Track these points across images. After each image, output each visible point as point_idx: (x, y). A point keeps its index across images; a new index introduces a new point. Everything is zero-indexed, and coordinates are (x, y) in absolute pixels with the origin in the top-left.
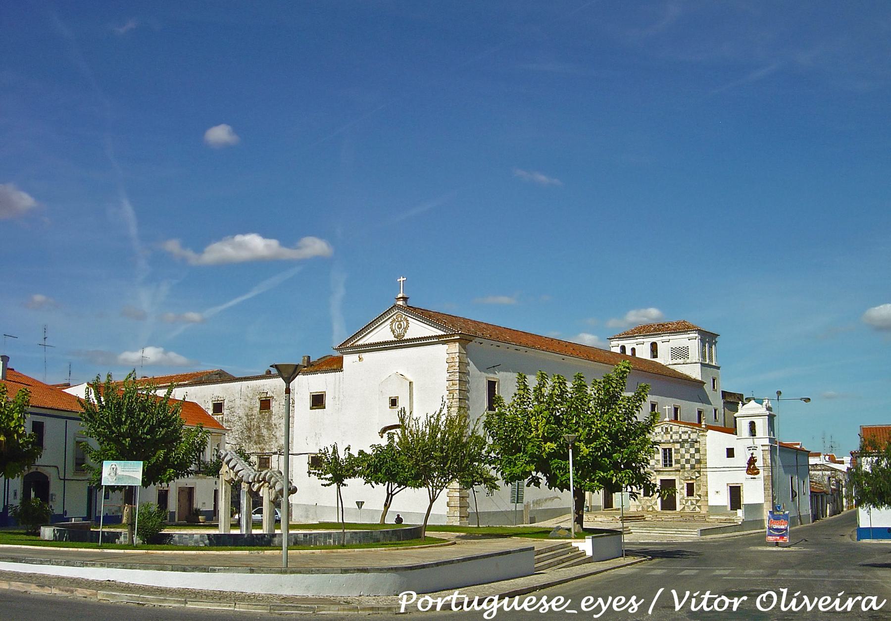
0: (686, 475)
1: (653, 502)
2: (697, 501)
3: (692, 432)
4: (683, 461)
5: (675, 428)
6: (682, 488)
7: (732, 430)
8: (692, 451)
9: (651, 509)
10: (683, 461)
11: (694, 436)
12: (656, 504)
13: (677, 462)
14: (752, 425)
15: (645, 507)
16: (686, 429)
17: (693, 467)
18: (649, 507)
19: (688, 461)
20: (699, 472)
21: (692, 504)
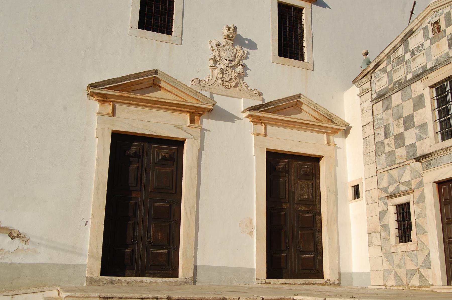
1: (421, 260)
15: (402, 274)
18: (411, 273)
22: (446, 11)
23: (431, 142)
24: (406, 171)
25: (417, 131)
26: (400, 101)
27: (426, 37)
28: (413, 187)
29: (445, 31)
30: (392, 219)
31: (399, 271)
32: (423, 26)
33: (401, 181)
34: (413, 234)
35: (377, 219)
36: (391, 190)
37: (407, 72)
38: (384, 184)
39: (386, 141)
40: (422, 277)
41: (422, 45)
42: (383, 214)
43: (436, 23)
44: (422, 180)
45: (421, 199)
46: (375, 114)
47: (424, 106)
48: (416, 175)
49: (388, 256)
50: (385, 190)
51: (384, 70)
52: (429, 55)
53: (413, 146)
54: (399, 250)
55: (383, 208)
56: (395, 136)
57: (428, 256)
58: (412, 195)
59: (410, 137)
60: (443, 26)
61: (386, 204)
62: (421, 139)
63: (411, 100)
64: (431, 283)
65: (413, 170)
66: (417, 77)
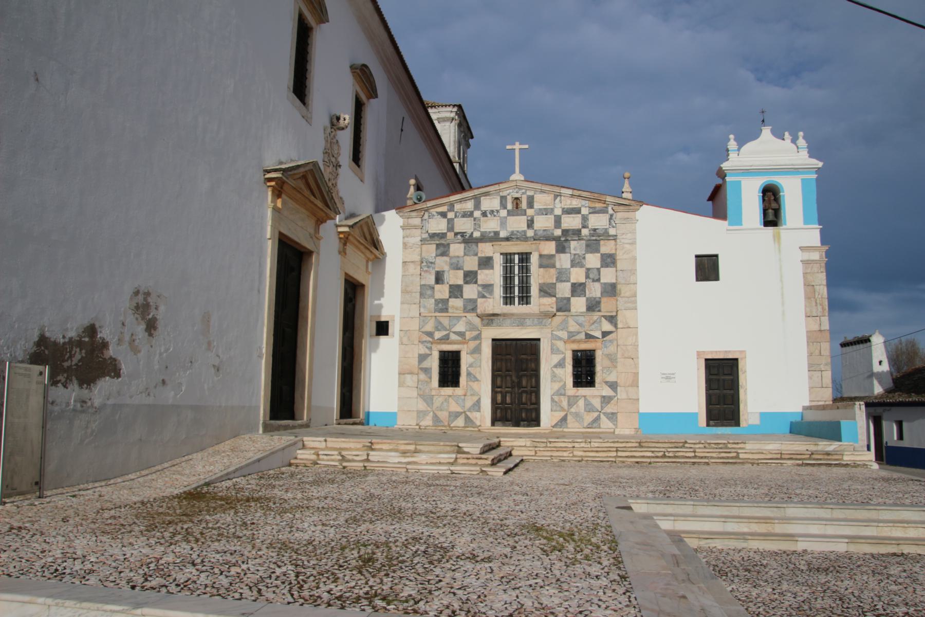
0: (573, 326)
1: (469, 403)
2: (606, 400)
3: (594, 211)
4: (564, 289)
5: (542, 200)
6: (561, 364)
7: (716, 201)
8: (593, 261)
9: (460, 422)
10: (564, 289)
11: (598, 221)
12: (477, 406)
13: (547, 291)
14: (771, 195)
15: (443, 415)
16: (575, 203)
17: (593, 306)
18: (457, 415)
19: (578, 289)
20: (612, 319)
21: (589, 408)
22: (530, 193)
23: (494, 303)
24: (461, 322)
25: (480, 289)
26: (462, 254)
27: (503, 205)
28: (467, 338)
29: (525, 211)
30: (434, 364)
31: (439, 414)
32: (501, 194)
33: (453, 330)
34: (463, 379)
35: (415, 362)
36: (438, 335)
37: (475, 229)
38: (429, 327)
39: (437, 287)
40: (468, 419)
41: (498, 211)
42: (422, 358)
43: (517, 199)
44: (480, 334)
45: (477, 350)
46: (423, 255)
47: (492, 268)
48: (472, 327)
49: (428, 399)
50: (430, 334)
51: (444, 215)
52: (503, 223)
53: (474, 301)
54: (443, 393)
55: (423, 350)
56: (450, 286)
57: (479, 401)
58: (465, 346)
59: (470, 291)
60: (524, 205)
61: (430, 349)
62: (484, 297)
63: (476, 258)
64: (478, 424)
65: (469, 323)
66: (484, 238)
